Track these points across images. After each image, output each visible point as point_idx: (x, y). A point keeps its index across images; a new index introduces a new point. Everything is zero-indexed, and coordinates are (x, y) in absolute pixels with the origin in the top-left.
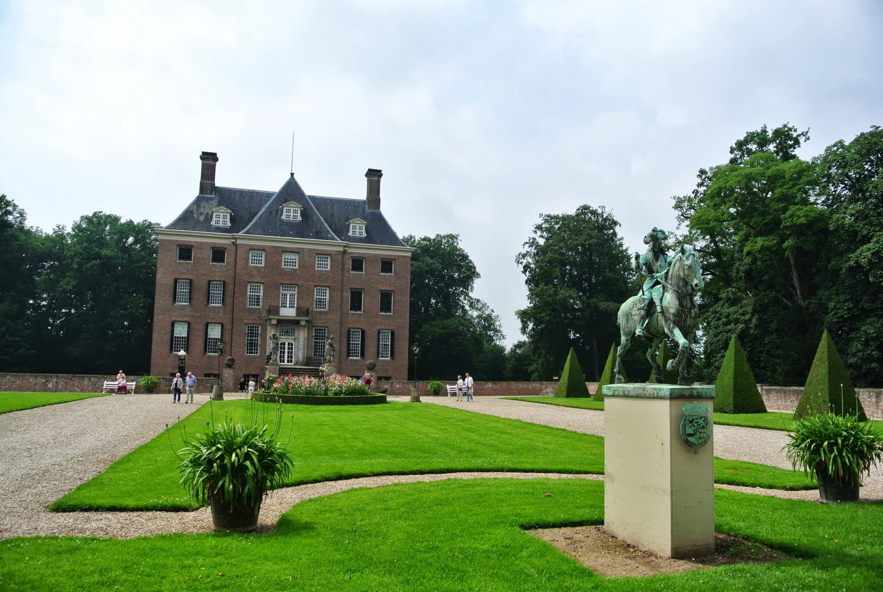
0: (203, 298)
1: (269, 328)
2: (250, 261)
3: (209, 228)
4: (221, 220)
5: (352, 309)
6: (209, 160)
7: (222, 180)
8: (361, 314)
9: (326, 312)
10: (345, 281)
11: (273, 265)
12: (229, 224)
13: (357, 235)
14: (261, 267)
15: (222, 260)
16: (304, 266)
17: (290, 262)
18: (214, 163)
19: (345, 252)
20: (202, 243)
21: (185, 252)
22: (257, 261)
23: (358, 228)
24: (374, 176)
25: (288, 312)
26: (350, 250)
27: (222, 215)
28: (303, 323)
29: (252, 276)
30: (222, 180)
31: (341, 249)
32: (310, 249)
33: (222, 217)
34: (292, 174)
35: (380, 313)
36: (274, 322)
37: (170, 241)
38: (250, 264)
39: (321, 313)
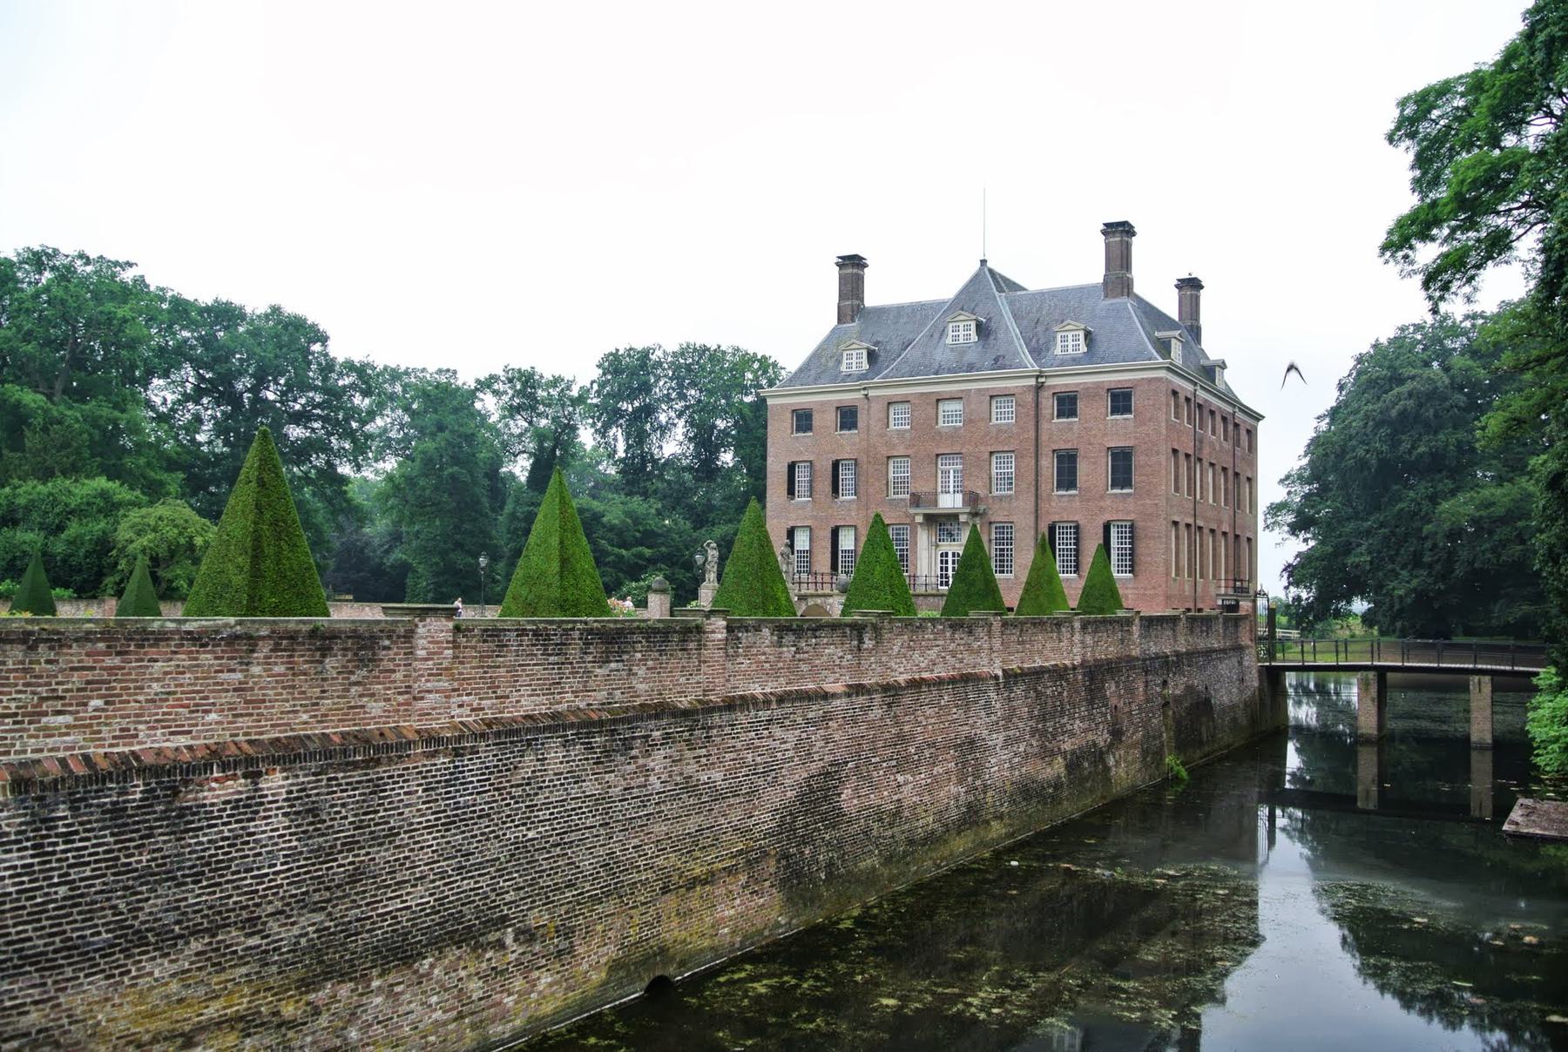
0: (828, 488)
1: (919, 529)
2: (892, 422)
3: (837, 377)
4: (854, 361)
5: (1059, 487)
6: (852, 266)
7: (876, 294)
8: (1074, 496)
9: (1010, 496)
10: (1044, 437)
11: (925, 428)
12: (866, 366)
13: (1070, 351)
14: (906, 431)
15: (853, 425)
16: (971, 421)
18: (855, 271)
19: (1039, 388)
20: (822, 403)
21: (804, 420)
23: (1070, 338)
24: (1119, 233)
25: (950, 501)
26: (1050, 382)
27: (854, 352)
28: (963, 518)
29: (894, 447)
31: (1032, 382)
32: (979, 390)
33: (856, 361)
34: (983, 262)
35: (1110, 491)
36: (919, 519)
37: (782, 406)
38: (892, 427)
39: (1001, 498)
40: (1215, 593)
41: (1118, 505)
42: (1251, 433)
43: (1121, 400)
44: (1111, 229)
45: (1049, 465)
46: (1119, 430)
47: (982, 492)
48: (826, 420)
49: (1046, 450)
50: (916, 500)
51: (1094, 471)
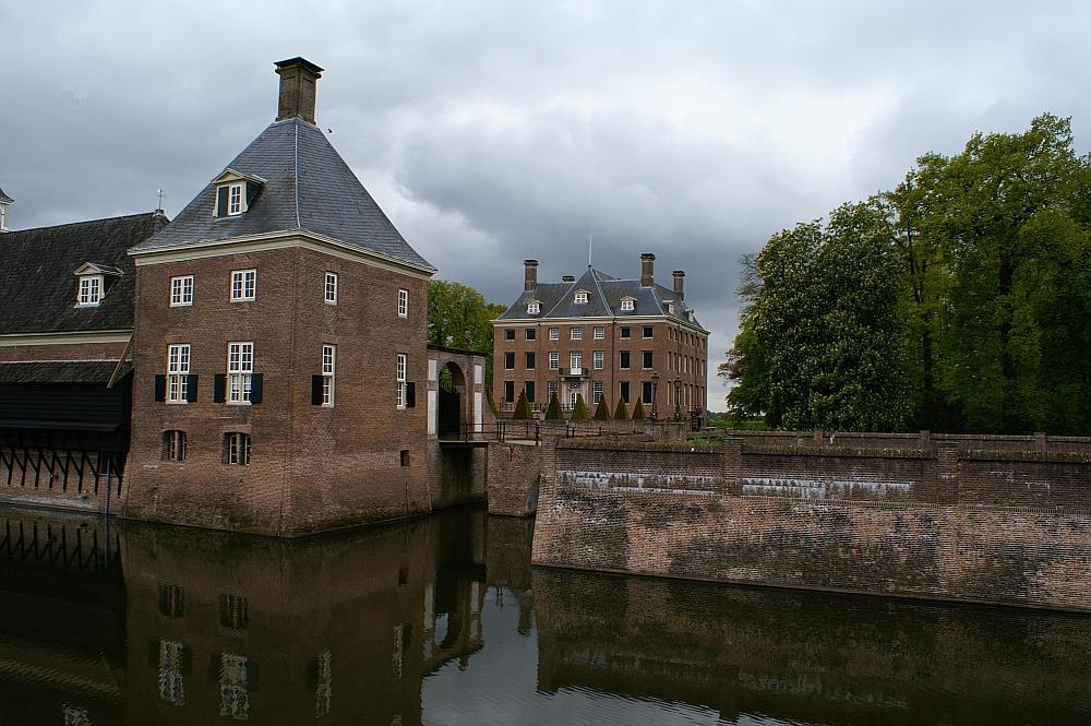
6: (531, 263)
7: (542, 277)
11: (565, 338)
12: (538, 311)
17: (575, 337)
22: (553, 337)
25: (576, 371)
30: (542, 277)
33: (534, 308)
36: (563, 379)
40: (688, 408)
41: (646, 374)
42: (705, 340)
43: (648, 331)
44: (645, 256)
45: (619, 358)
46: (647, 343)
47: (589, 368)
48: (519, 335)
49: (617, 350)
50: (561, 370)
51: (637, 360)
